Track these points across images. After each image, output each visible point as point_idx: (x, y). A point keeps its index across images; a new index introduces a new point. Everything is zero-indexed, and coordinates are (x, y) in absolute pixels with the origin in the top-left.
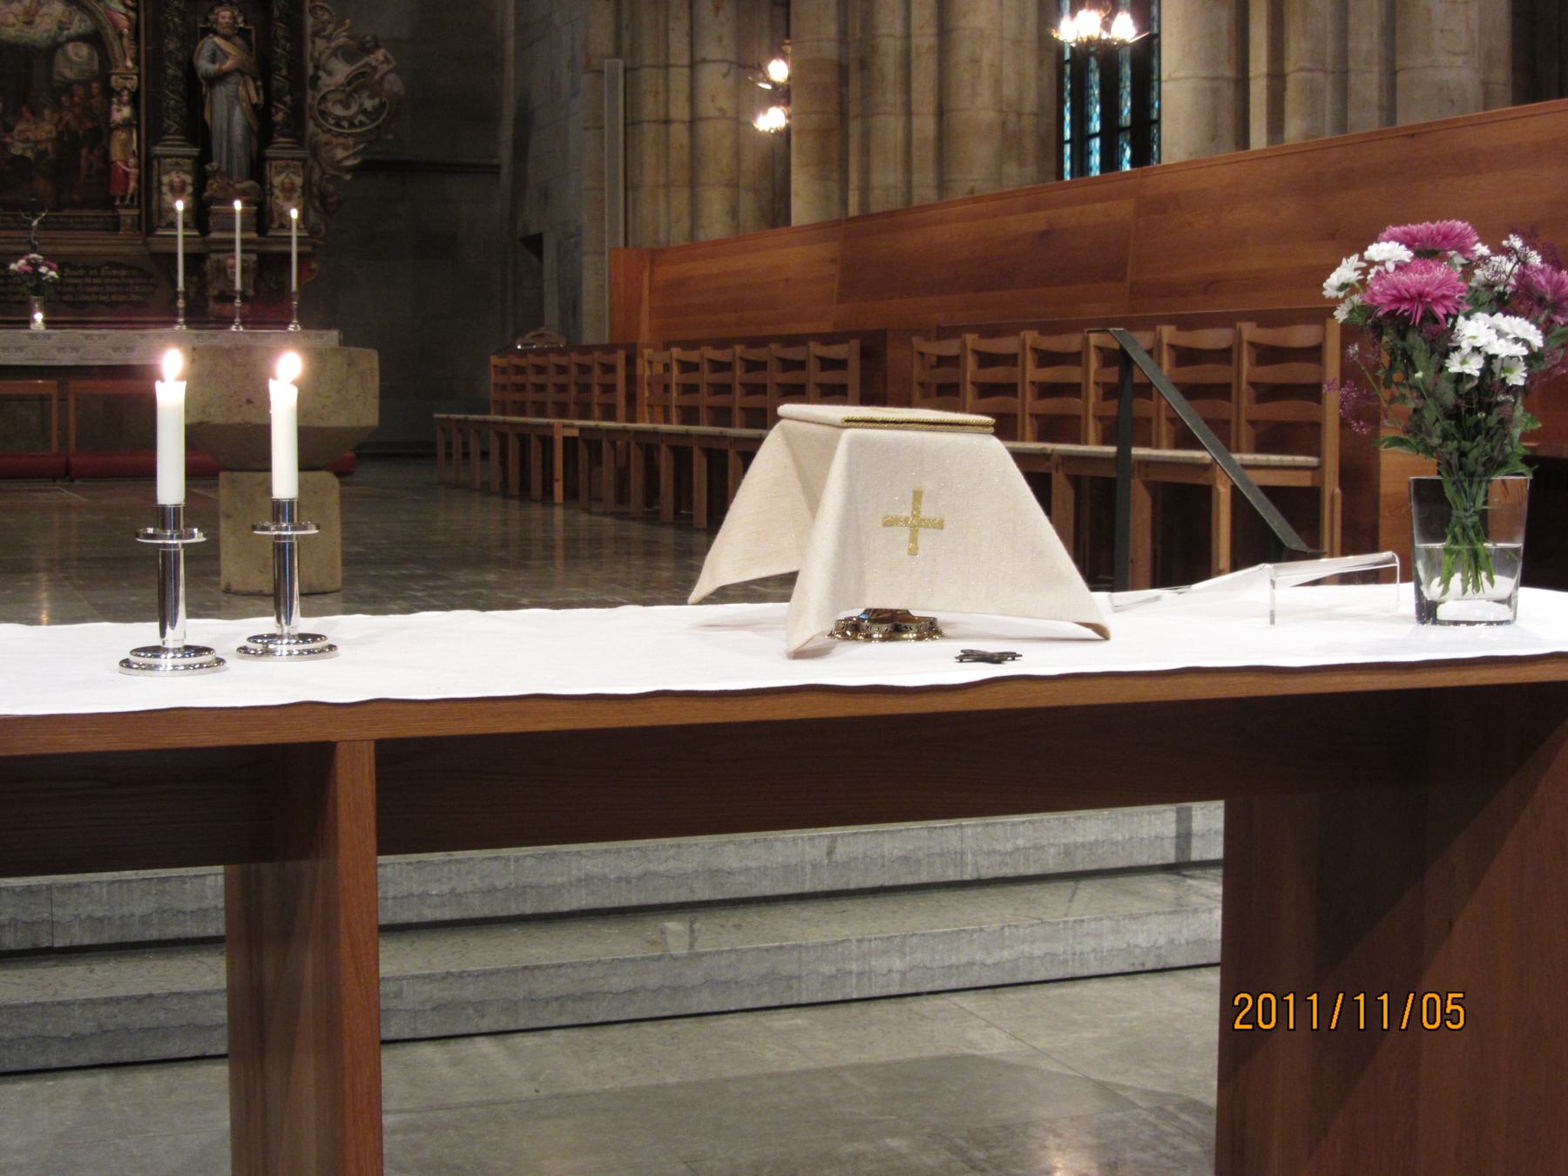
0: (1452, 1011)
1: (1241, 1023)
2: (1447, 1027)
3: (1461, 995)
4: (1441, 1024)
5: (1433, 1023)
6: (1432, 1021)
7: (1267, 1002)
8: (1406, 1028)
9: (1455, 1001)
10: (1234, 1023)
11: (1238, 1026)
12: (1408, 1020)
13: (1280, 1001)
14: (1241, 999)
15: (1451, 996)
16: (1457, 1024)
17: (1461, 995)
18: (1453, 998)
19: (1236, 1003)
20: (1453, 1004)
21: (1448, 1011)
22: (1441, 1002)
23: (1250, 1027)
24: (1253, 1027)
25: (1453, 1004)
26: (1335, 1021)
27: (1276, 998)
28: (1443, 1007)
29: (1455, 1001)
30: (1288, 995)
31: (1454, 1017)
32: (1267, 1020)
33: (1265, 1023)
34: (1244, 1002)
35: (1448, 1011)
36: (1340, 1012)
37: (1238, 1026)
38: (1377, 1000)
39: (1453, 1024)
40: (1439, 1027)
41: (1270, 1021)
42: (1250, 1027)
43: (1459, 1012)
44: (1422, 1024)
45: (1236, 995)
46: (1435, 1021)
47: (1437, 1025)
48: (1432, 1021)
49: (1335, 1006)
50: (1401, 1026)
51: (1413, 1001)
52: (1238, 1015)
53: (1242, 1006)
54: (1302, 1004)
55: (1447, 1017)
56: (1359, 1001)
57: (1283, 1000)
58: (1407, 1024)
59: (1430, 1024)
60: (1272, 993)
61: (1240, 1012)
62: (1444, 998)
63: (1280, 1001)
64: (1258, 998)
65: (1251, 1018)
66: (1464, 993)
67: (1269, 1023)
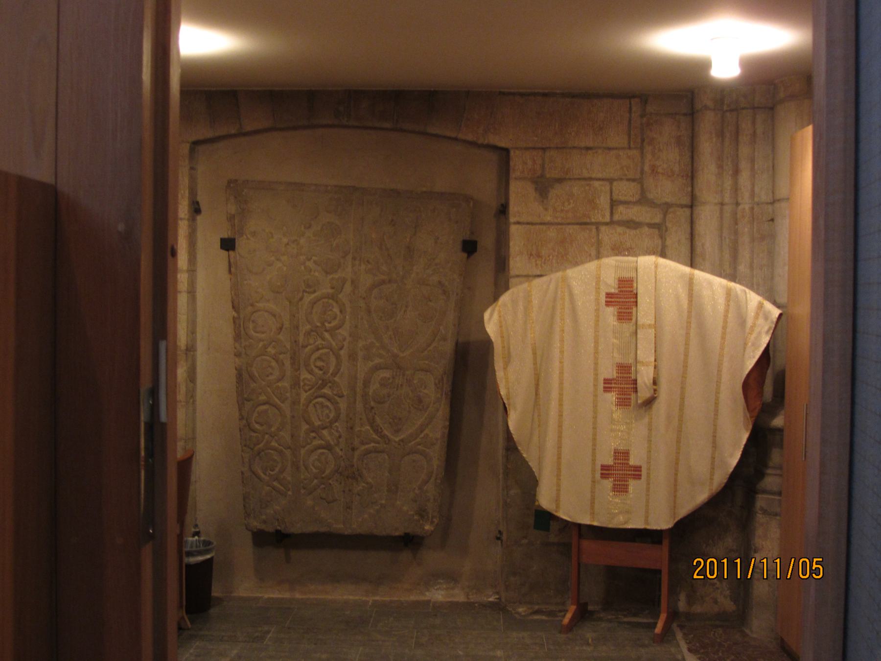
0: (816, 568)
1: (697, 575)
2: (813, 577)
3: (821, 559)
4: (810, 575)
5: (805, 575)
6: (804, 574)
7: (712, 563)
8: (790, 578)
9: (817, 563)
10: (693, 575)
11: (695, 577)
12: (791, 573)
13: (719, 561)
14: (697, 561)
15: (815, 560)
16: (818, 575)
17: (821, 559)
18: (817, 561)
19: (695, 564)
20: (816, 564)
21: (814, 568)
22: (810, 563)
23: (702, 577)
24: (704, 577)
25: (816, 564)
26: (750, 574)
27: (717, 561)
28: (811, 566)
29: (817, 563)
30: (724, 559)
31: (817, 572)
32: (712, 573)
33: (711, 575)
34: (699, 563)
35: (814, 568)
36: (750, 568)
37: (695, 577)
38: (734, 562)
39: (817, 575)
40: (809, 577)
41: (714, 574)
42: (702, 577)
43: (820, 569)
44: (799, 575)
45: (695, 559)
46: (806, 574)
47: (807, 576)
48: (804, 574)
49: (750, 565)
50: (787, 576)
51: (794, 562)
52: (695, 571)
53: (698, 566)
54: (732, 565)
55: (813, 572)
56: (724, 563)
57: (721, 562)
58: (791, 575)
59: (803, 575)
60: (715, 558)
61: (697, 569)
62: (811, 561)
63: (719, 561)
64: (707, 561)
65: (703, 572)
66: (823, 558)
67: (713, 575)
